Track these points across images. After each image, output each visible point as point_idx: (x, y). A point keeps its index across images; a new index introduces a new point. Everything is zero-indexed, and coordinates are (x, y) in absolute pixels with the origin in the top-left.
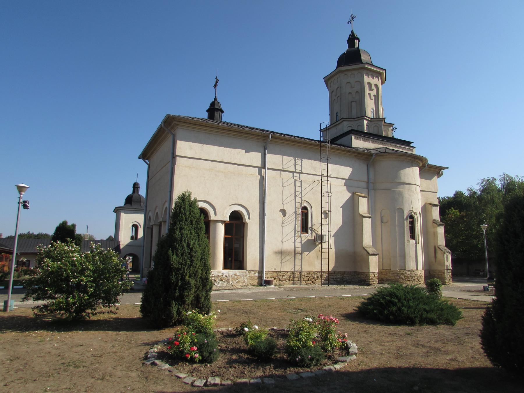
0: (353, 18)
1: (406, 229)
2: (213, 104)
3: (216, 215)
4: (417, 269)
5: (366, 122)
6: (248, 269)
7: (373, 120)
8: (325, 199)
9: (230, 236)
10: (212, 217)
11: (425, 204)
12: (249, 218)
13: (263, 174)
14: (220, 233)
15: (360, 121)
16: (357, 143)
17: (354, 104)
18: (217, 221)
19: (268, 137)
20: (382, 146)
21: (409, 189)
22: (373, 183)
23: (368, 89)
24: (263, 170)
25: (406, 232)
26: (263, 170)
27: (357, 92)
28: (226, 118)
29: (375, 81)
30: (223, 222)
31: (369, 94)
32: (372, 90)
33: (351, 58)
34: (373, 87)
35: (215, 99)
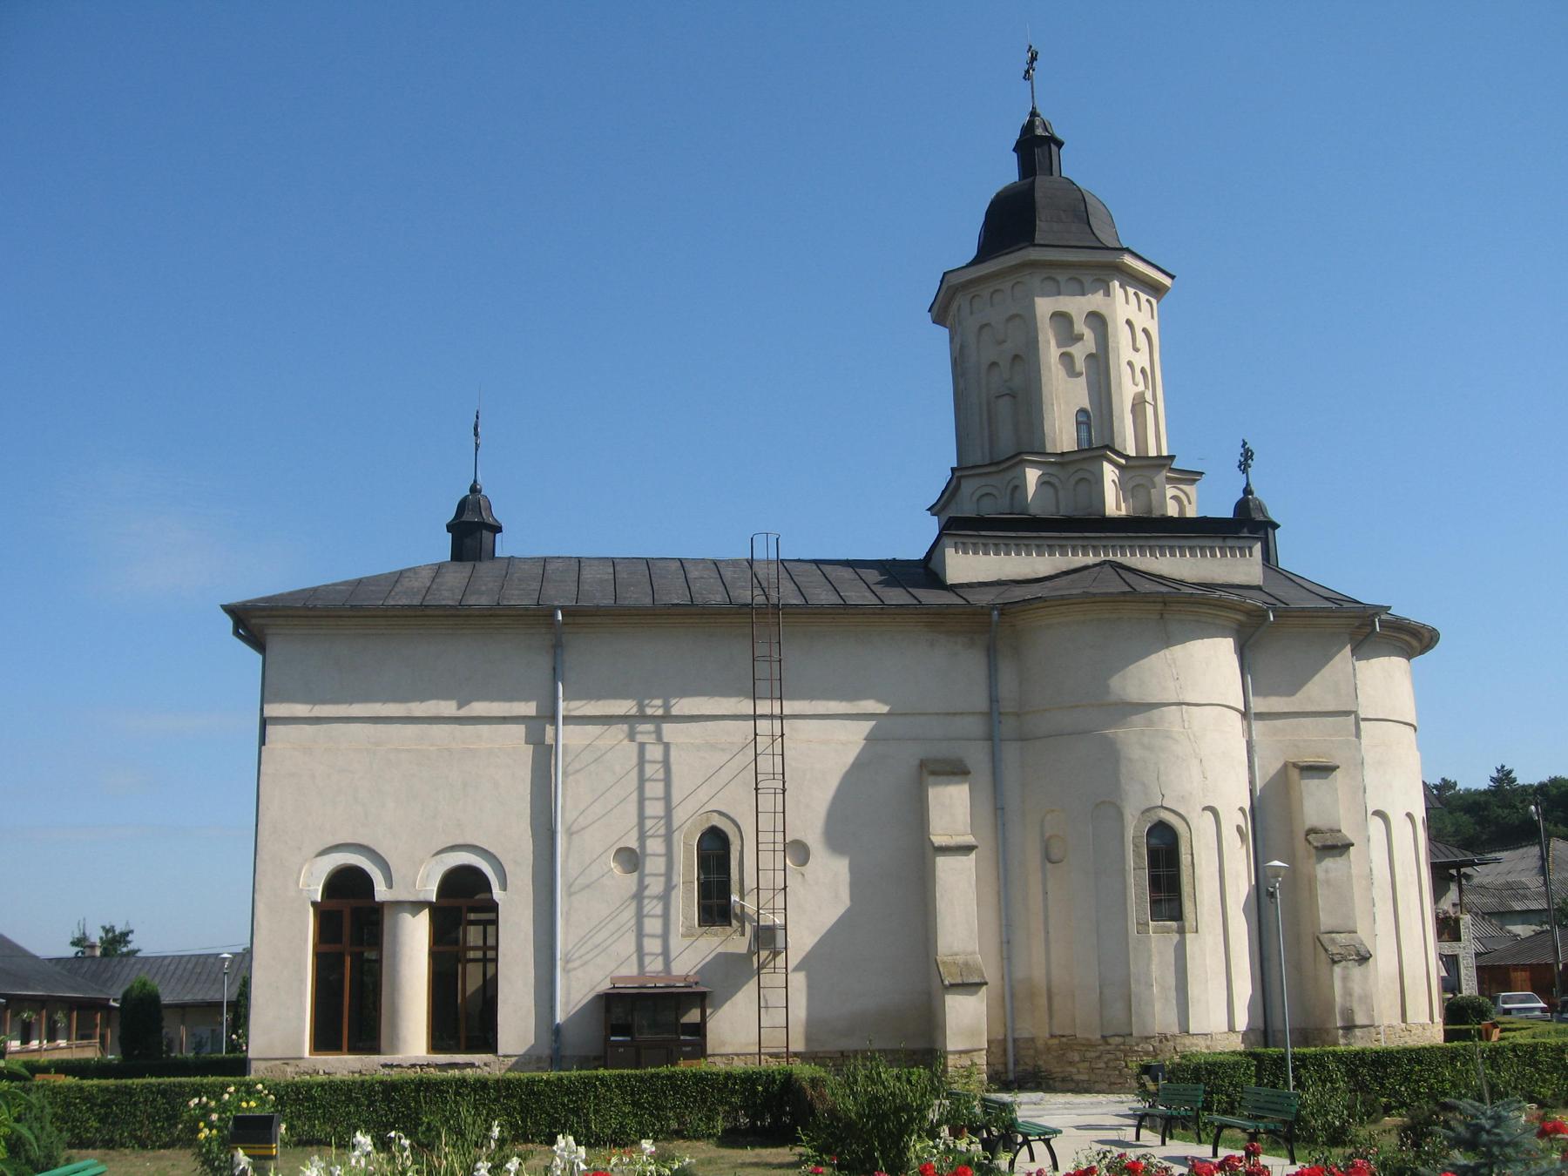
0: (1034, 58)
1: (1131, 881)
2: (462, 506)
3: (390, 885)
4: (1185, 1031)
5: (1032, 475)
6: (501, 1051)
7: (1067, 459)
8: (766, 802)
9: (348, 960)
10: (381, 892)
11: (1285, 765)
12: (504, 887)
13: (549, 740)
14: (413, 943)
15: (1009, 475)
16: (966, 566)
17: (1004, 405)
18: (399, 905)
19: (554, 615)
20: (1091, 559)
21: (1150, 723)
22: (1018, 715)
23: (1053, 342)
24: (549, 729)
25: (1132, 892)
26: (549, 729)
27: (1016, 357)
28: (505, 546)
29: (1077, 306)
30: (416, 906)
31: (1067, 358)
32: (1080, 338)
33: (1010, 223)
34: (1080, 326)
35: (474, 489)
